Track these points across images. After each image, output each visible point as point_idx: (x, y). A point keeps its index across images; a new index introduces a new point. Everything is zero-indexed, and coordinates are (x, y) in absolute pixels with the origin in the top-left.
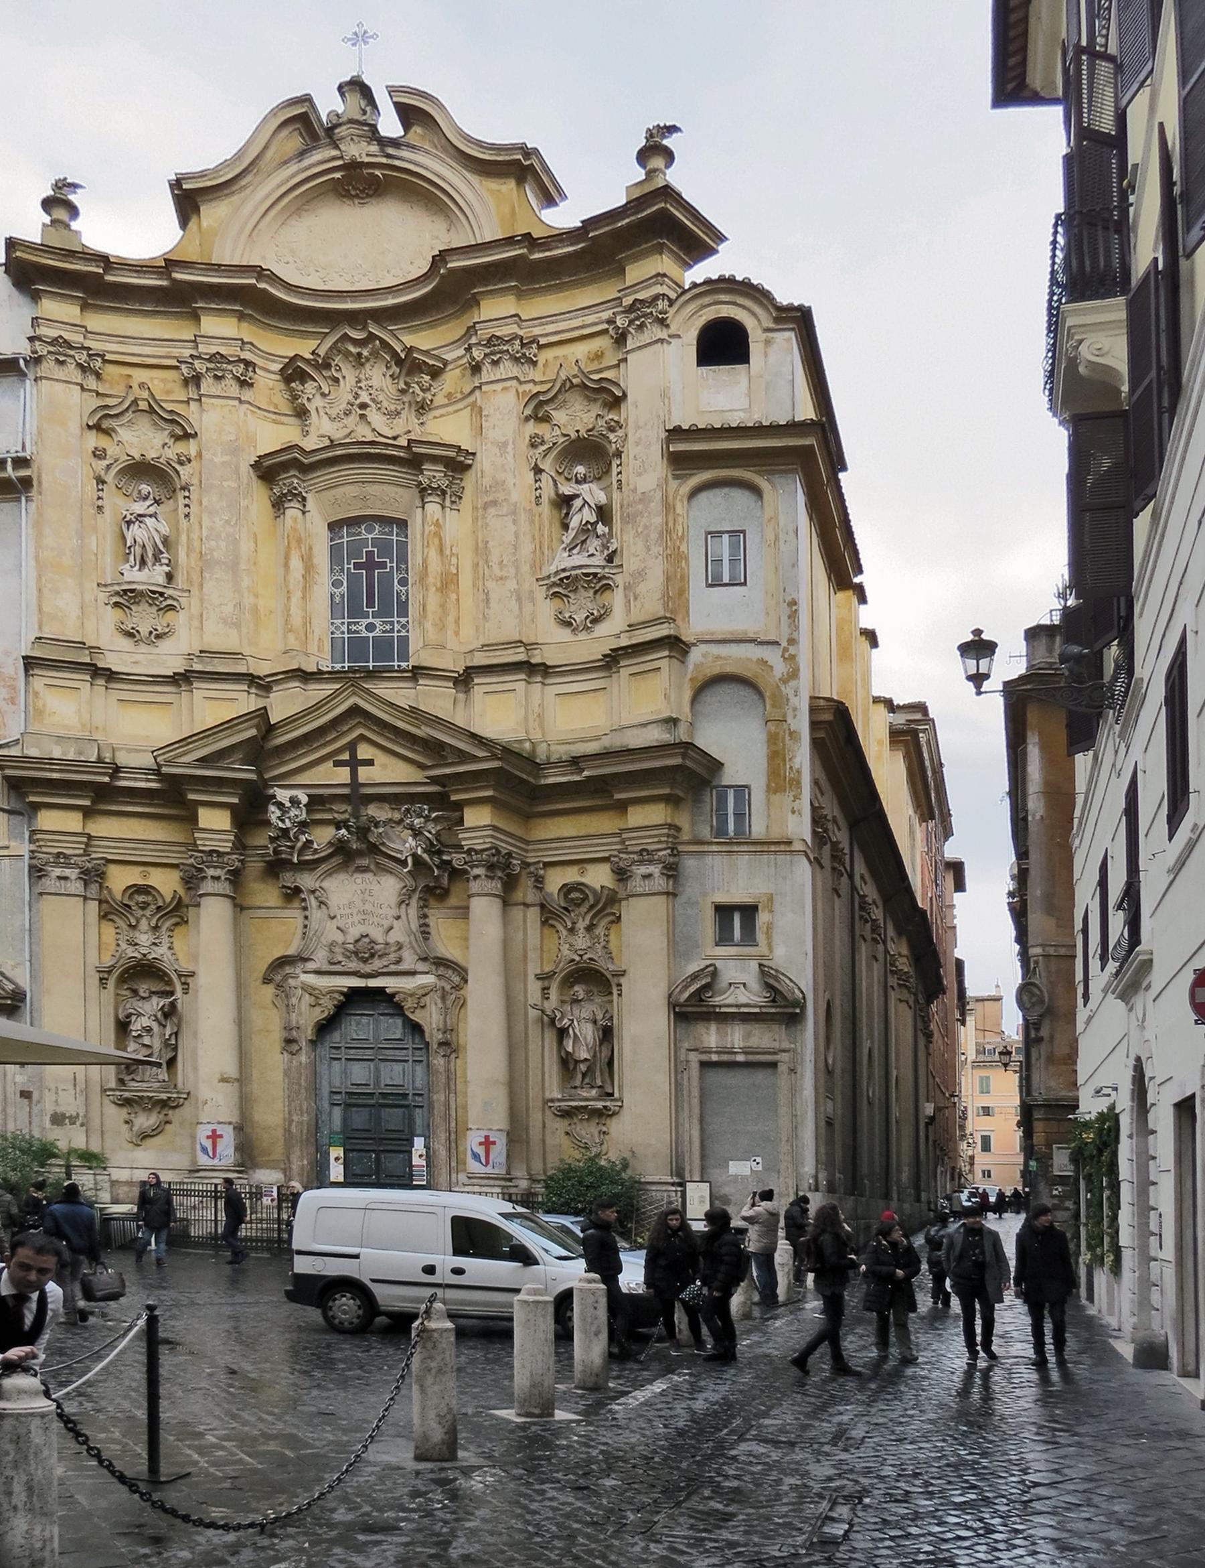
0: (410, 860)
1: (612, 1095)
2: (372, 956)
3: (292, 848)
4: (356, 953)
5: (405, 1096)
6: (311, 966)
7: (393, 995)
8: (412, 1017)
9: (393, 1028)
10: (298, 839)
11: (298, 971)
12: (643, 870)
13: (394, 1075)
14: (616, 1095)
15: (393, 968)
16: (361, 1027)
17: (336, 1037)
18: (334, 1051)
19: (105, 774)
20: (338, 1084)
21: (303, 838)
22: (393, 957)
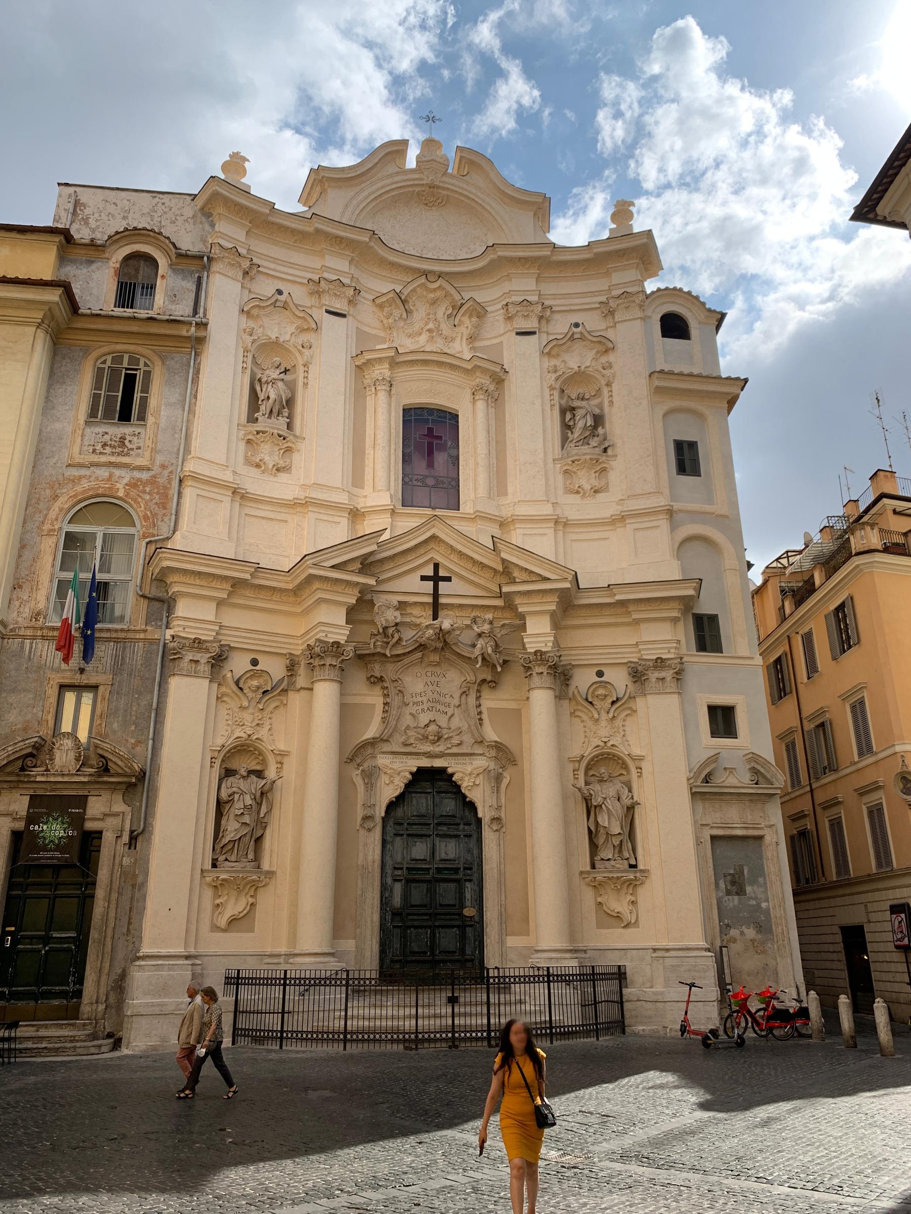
0: (480, 659)
1: (635, 866)
2: (439, 738)
3: (388, 643)
4: (425, 738)
5: (456, 870)
6: (386, 747)
7: (452, 775)
8: (467, 793)
9: (449, 805)
10: (393, 636)
11: (376, 751)
12: (657, 674)
13: (449, 850)
14: (641, 866)
15: (455, 750)
16: (421, 804)
17: (399, 812)
18: (398, 827)
19: (246, 572)
20: (399, 859)
21: (396, 636)
22: (455, 741)
